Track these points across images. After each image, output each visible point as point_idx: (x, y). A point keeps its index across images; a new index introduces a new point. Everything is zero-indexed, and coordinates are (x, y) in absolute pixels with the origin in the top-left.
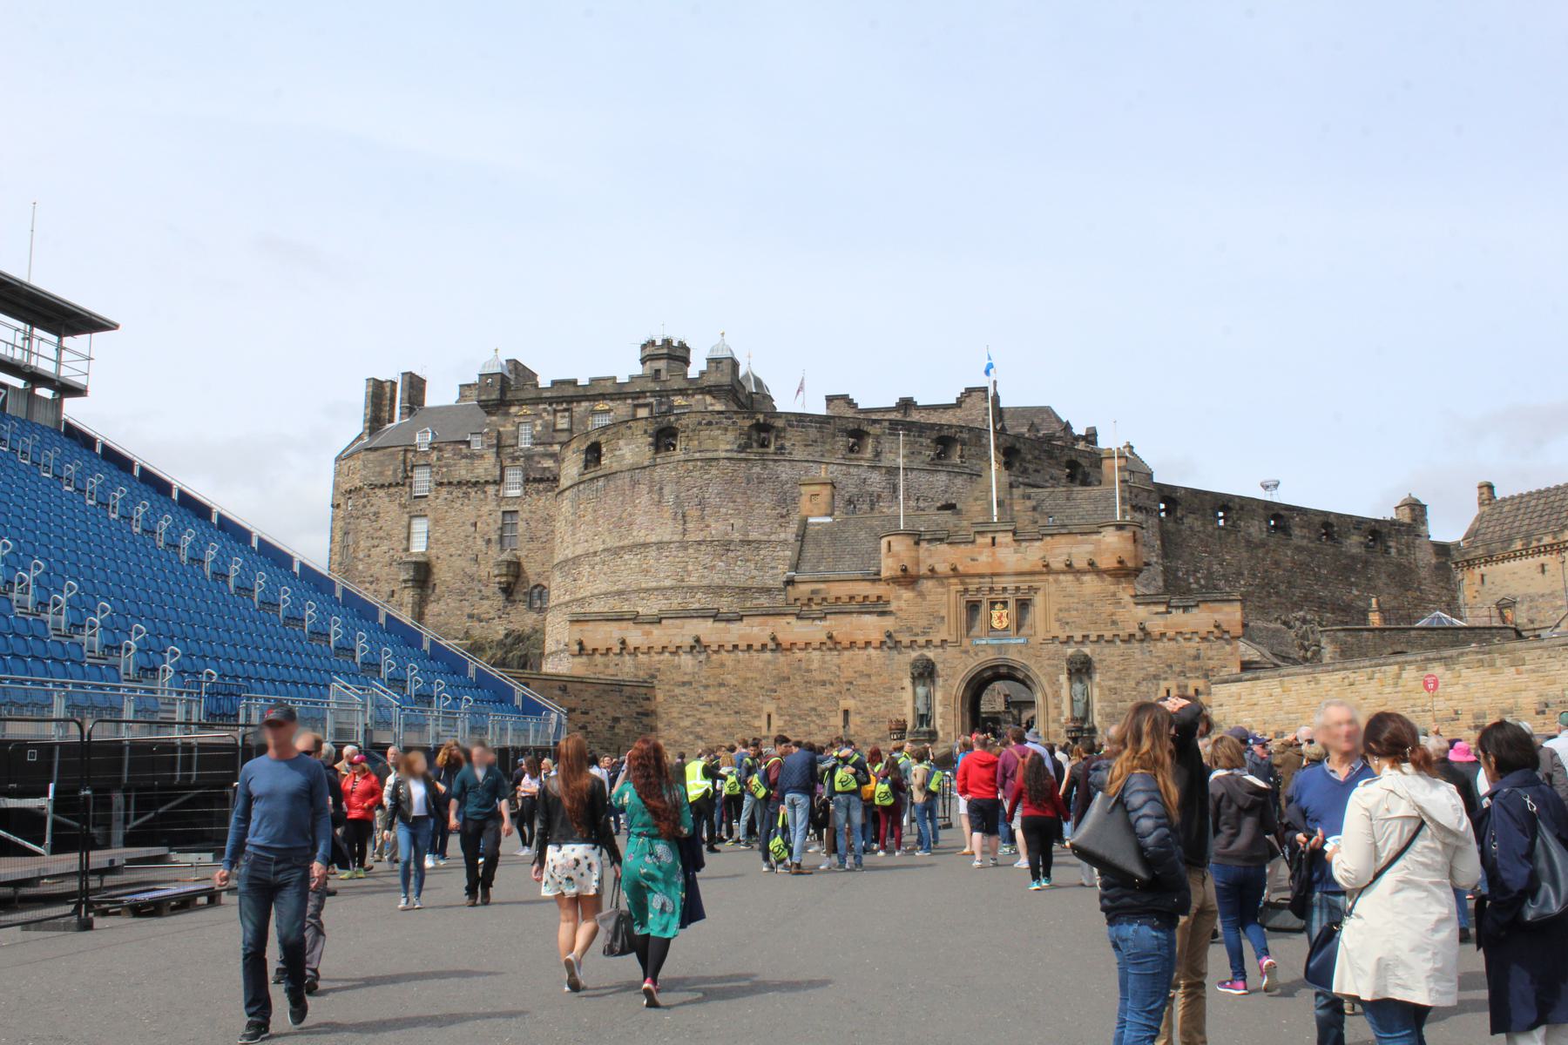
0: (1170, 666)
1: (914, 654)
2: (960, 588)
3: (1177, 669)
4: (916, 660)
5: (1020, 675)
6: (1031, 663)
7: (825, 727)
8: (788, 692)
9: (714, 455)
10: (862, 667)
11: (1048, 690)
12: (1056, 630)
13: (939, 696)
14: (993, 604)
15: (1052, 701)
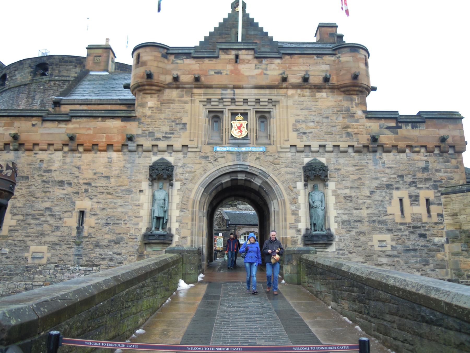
0: (401, 177)
1: (155, 159)
2: (204, 98)
3: (408, 179)
4: (155, 164)
5: (258, 182)
6: (269, 170)
7: (58, 228)
8: (24, 191)
9: (68, 79)
10: (101, 169)
11: (286, 197)
12: (294, 139)
13: (176, 199)
14: (234, 115)
15: (290, 208)
